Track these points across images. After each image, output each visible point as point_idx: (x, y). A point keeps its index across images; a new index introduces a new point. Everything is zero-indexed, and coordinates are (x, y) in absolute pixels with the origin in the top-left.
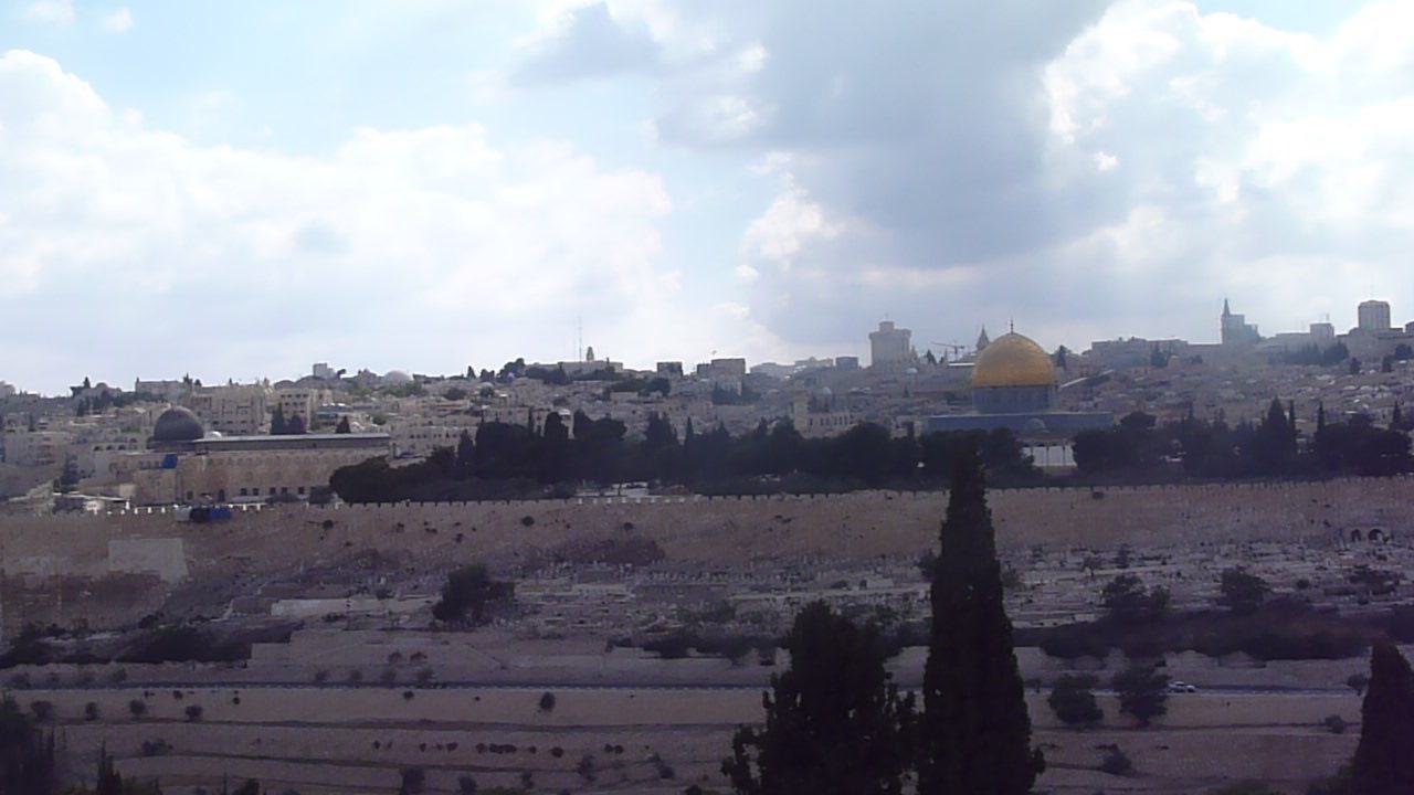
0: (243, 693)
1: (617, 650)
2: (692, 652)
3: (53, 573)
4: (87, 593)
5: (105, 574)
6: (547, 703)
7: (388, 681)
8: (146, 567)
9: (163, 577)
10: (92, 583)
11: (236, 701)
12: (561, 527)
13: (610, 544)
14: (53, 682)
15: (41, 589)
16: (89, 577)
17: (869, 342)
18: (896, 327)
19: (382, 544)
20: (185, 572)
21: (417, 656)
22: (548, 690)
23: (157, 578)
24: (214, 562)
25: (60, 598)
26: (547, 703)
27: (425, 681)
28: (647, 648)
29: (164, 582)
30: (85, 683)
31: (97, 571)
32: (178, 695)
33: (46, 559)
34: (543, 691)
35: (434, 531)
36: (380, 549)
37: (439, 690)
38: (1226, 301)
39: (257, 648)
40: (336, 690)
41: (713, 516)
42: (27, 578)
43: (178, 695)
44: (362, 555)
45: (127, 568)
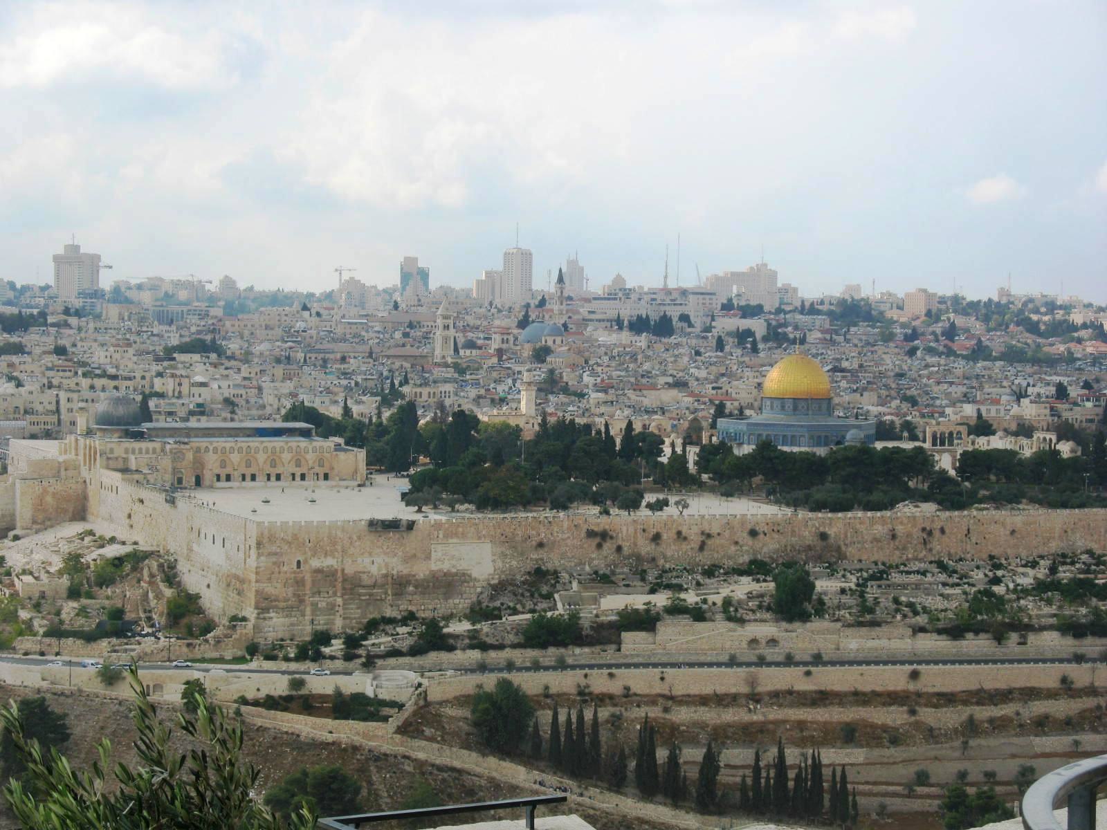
0: (669, 671)
1: (921, 635)
2: (970, 635)
3: (384, 572)
4: (411, 588)
5: (427, 573)
6: (915, 675)
7: (789, 661)
8: (463, 566)
9: (473, 576)
10: (417, 580)
11: (662, 679)
12: (776, 536)
13: (809, 548)
14: (510, 666)
15: (374, 586)
16: (414, 576)
17: (52, 264)
18: (82, 251)
19: (646, 548)
20: (491, 571)
21: (773, 642)
22: (915, 666)
23: (470, 576)
24: (514, 563)
25: (390, 592)
26: (915, 675)
27: (818, 660)
28: (940, 632)
29: (475, 579)
30: (536, 667)
31: (421, 570)
32: (611, 675)
33: (379, 560)
34: (908, 668)
35: (685, 539)
36: (643, 553)
37: (829, 668)
38: (560, 270)
39: (626, 636)
40: (773, 669)
41: (880, 528)
42: (364, 577)
43: (611, 675)
44: (629, 557)
45: (446, 566)
